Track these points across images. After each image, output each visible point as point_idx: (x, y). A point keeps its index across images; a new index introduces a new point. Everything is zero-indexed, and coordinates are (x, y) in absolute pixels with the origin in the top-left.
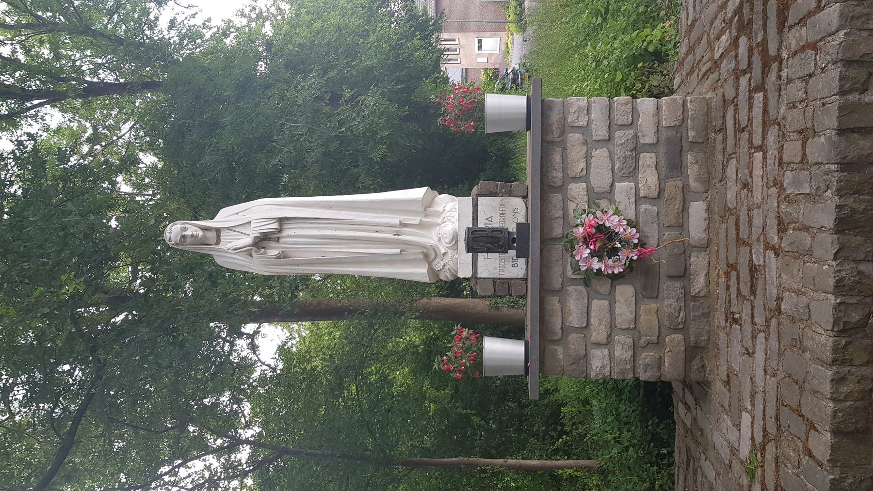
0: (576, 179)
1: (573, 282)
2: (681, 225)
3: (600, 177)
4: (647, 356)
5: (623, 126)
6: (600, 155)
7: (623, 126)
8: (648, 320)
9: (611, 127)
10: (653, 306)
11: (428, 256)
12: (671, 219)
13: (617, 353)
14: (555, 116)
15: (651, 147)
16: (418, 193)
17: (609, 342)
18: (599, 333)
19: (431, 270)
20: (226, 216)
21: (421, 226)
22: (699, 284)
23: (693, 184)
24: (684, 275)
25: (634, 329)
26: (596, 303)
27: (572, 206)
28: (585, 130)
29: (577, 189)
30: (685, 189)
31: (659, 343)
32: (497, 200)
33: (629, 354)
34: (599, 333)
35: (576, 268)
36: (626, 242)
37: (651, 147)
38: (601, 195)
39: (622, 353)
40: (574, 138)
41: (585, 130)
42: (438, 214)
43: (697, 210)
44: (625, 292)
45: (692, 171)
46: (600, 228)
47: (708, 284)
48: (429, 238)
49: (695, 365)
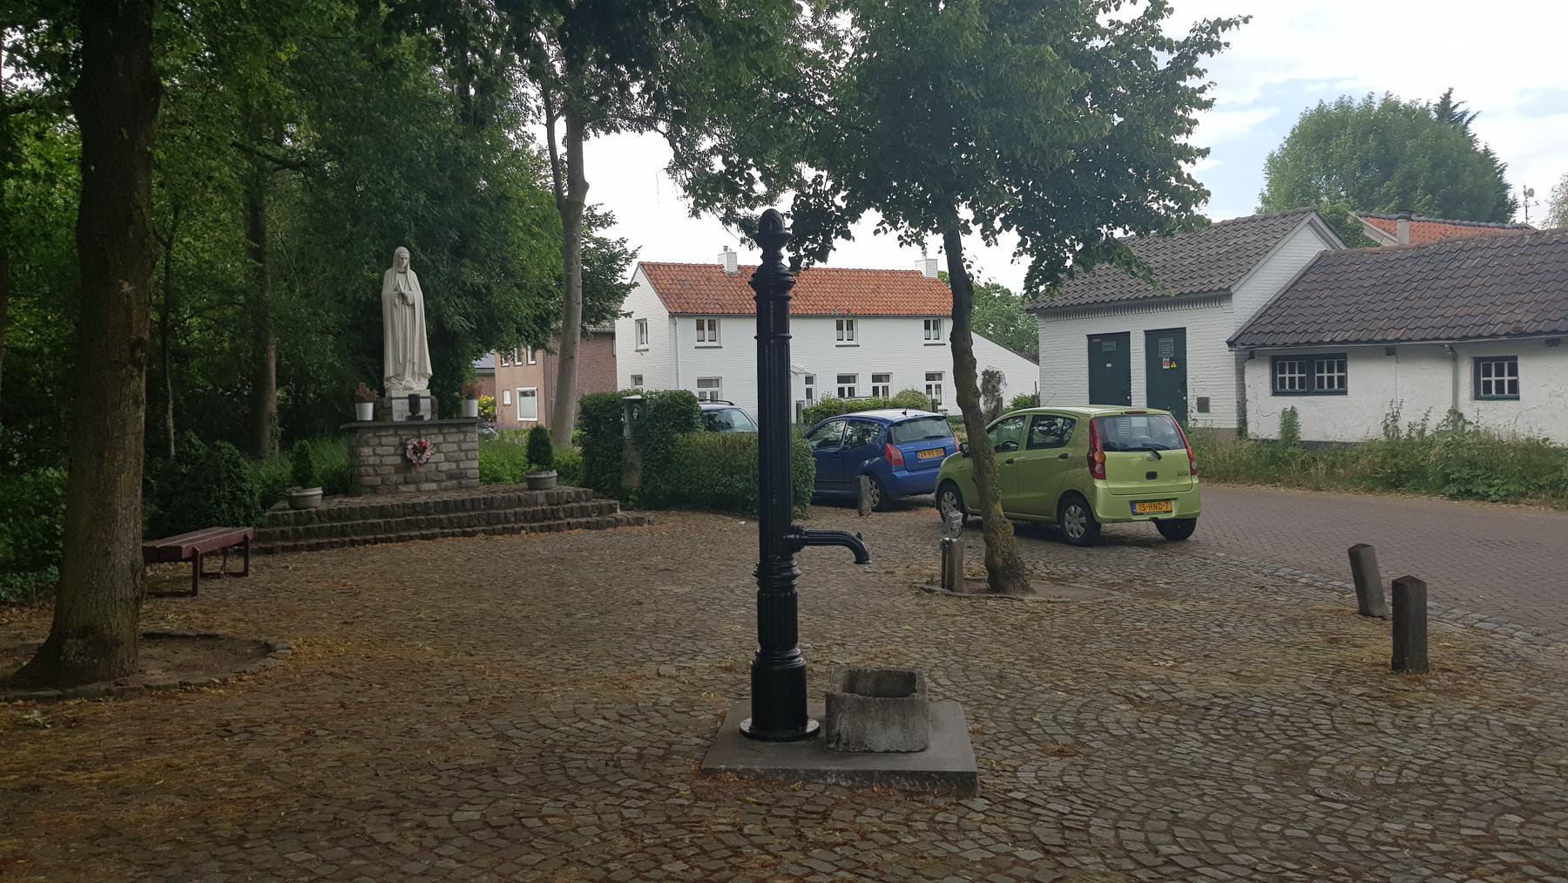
0: (444, 438)
1: (401, 439)
2: (427, 480)
3: (445, 447)
4: (371, 471)
5: (466, 455)
6: (455, 447)
7: (466, 455)
8: (386, 470)
9: (466, 451)
10: (393, 471)
11: (399, 376)
12: (429, 476)
13: (371, 458)
14: (470, 428)
15: (458, 466)
16: (430, 371)
17: (375, 455)
18: (379, 450)
19: (391, 378)
20: (412, 275)
21: (413, 372)
22: (403, 488)
23: (444, 484)
24: (406, 483)
25: (382, 465)
26: (392, 449)
27: (433, 437)
28: (465, 441)
29: (440, 439)
30: (442, 481)
31: (377, 474)
32: (429, 407)
33: (371, 463)
34: (379, 450)
35: (407, 439)
36: (420, 458)
37: (458, 466)
38: (438, 449)
39: (372, 460)
40: (462, 436)
41: (465, 441)
42: (419, 380)
43: (434, 486)
44: (398, 460)
45: (449, 483)
46: (425, 448)
47: (404, 492)
48: (408, 377)
49: (369, 490)
